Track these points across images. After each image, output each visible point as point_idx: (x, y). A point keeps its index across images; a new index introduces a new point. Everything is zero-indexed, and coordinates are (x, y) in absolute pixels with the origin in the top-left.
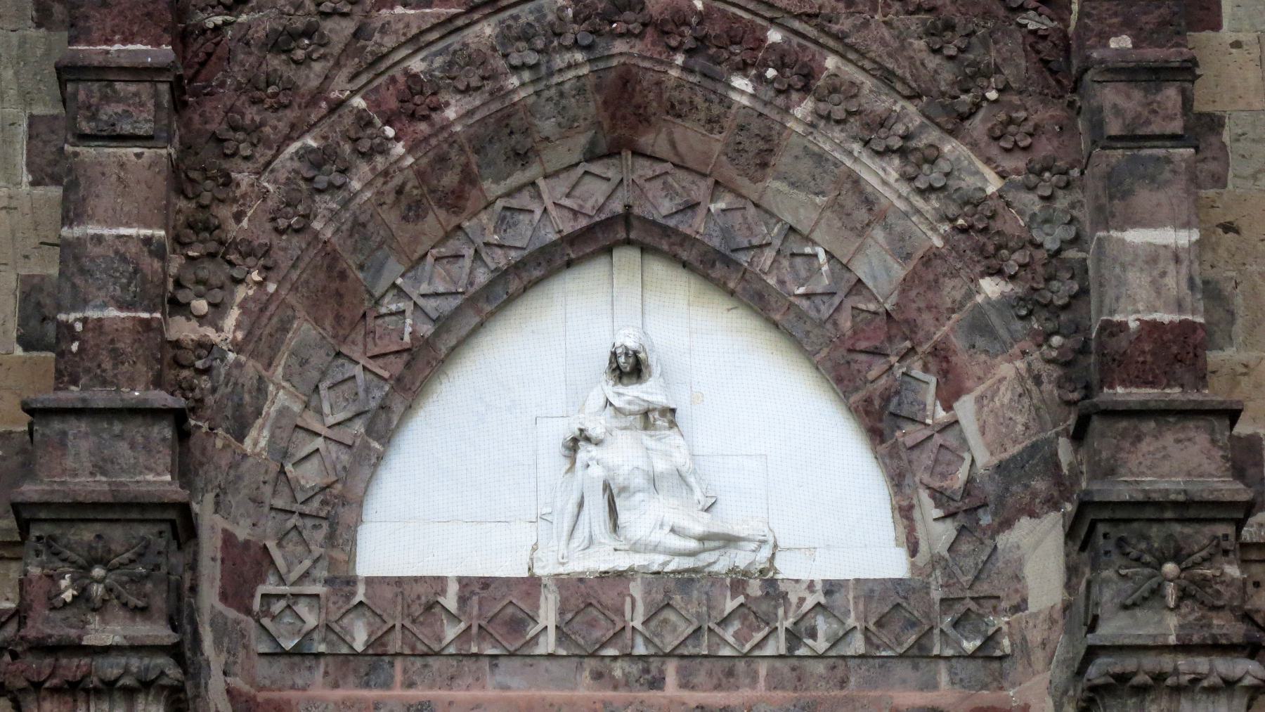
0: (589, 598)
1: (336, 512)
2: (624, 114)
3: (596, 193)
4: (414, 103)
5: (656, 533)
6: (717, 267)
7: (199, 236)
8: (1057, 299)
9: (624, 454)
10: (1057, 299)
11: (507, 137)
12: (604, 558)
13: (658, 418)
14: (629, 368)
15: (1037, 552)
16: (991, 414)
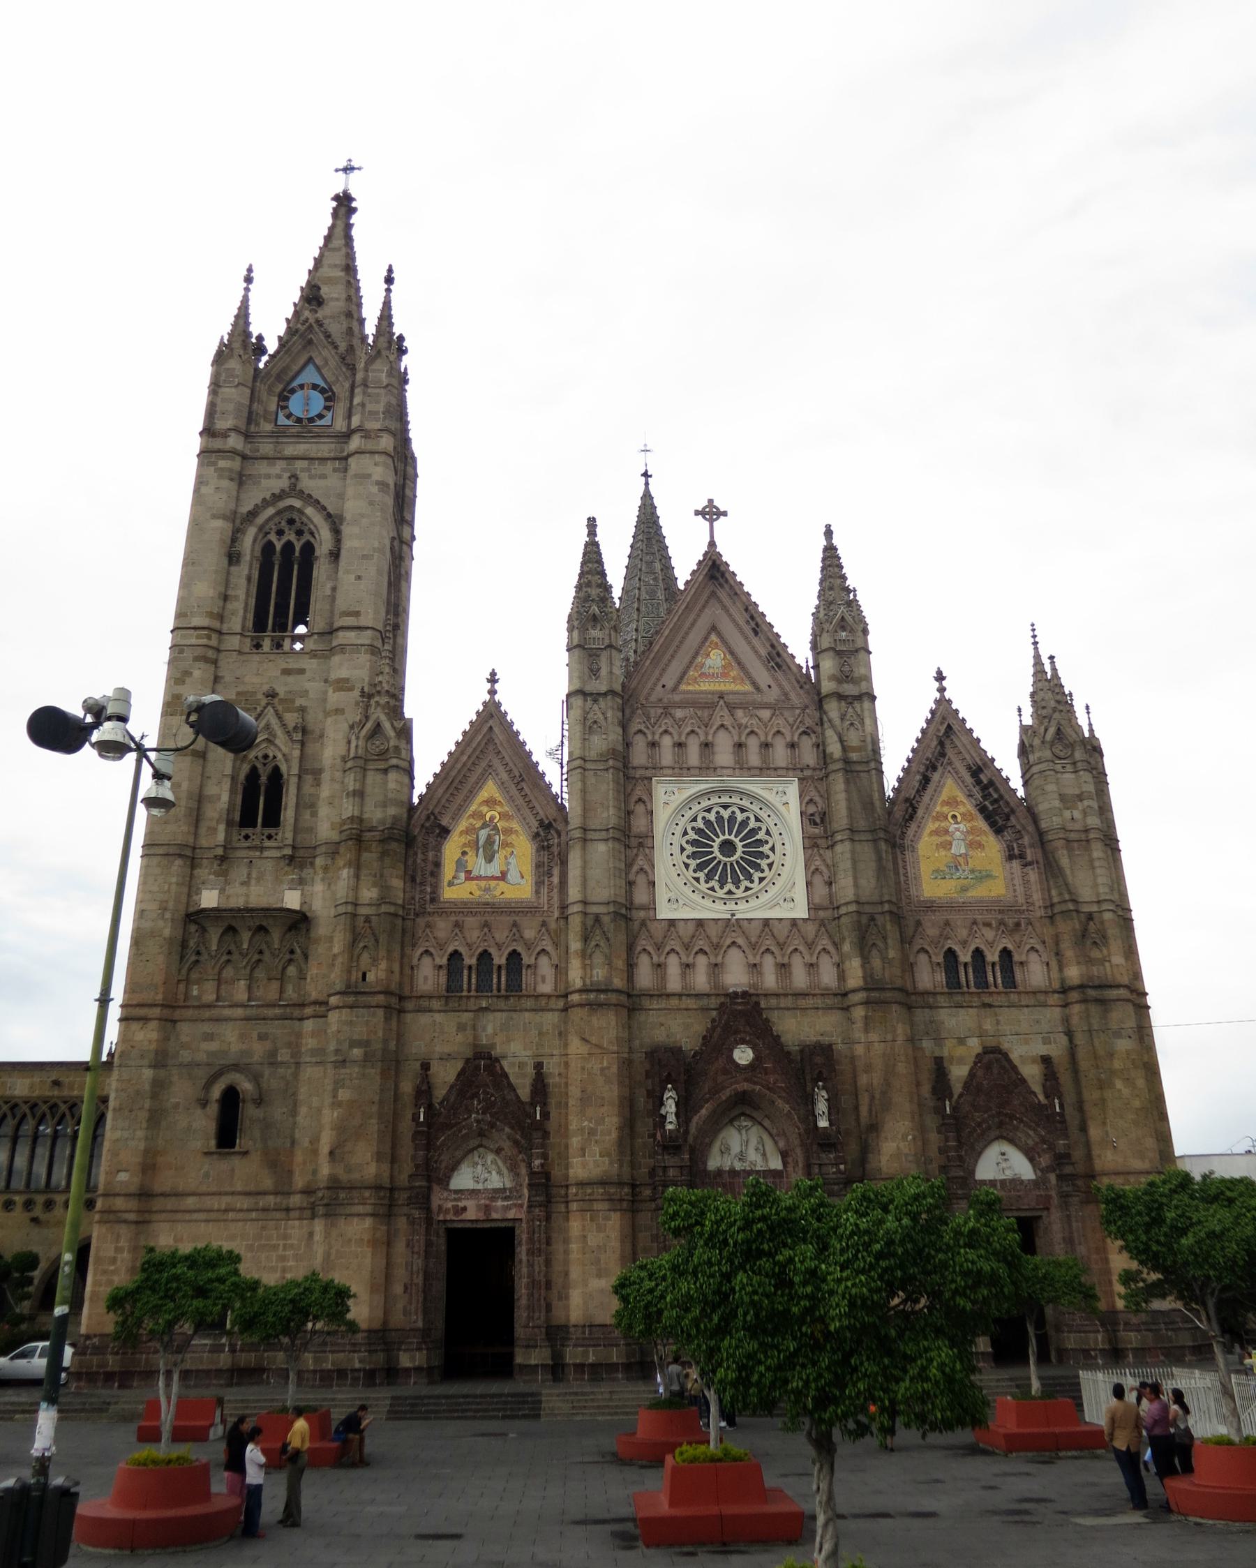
0: (1003, 1182)
1: (973, 1172)
2: (1001, 1125)
3: (997, 1133)
4: (979, 1125)
5: (1008, 1174)
6: (1012, 1141)
7: (960, 1144)
8: (1052, 1147)
9: (1004, 1165)
10: (1052, 1147)
11: (989, 1128)
12: (1003, 1177)
13: (1006, 1160)
14: (1003, 1154)
15: (1053, 1178)
16: (1045, 1160)
